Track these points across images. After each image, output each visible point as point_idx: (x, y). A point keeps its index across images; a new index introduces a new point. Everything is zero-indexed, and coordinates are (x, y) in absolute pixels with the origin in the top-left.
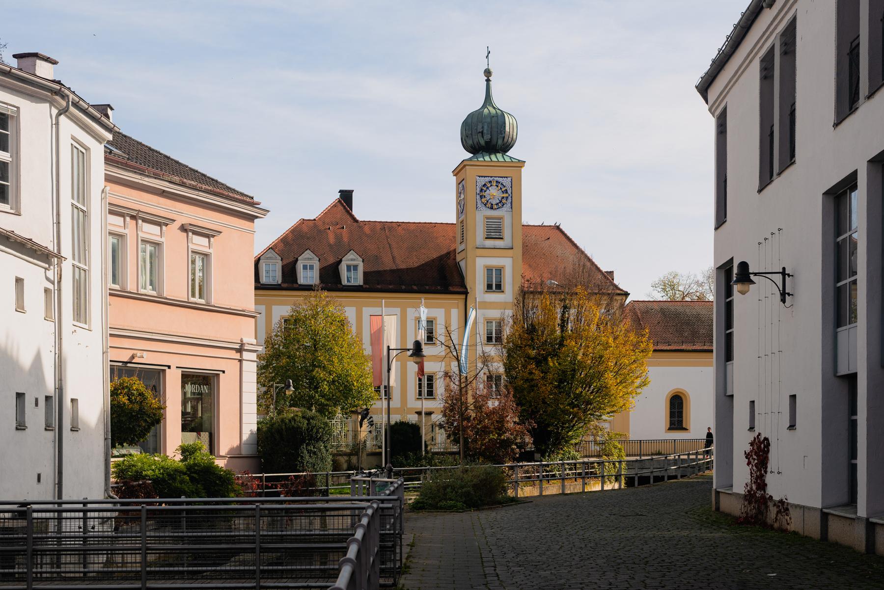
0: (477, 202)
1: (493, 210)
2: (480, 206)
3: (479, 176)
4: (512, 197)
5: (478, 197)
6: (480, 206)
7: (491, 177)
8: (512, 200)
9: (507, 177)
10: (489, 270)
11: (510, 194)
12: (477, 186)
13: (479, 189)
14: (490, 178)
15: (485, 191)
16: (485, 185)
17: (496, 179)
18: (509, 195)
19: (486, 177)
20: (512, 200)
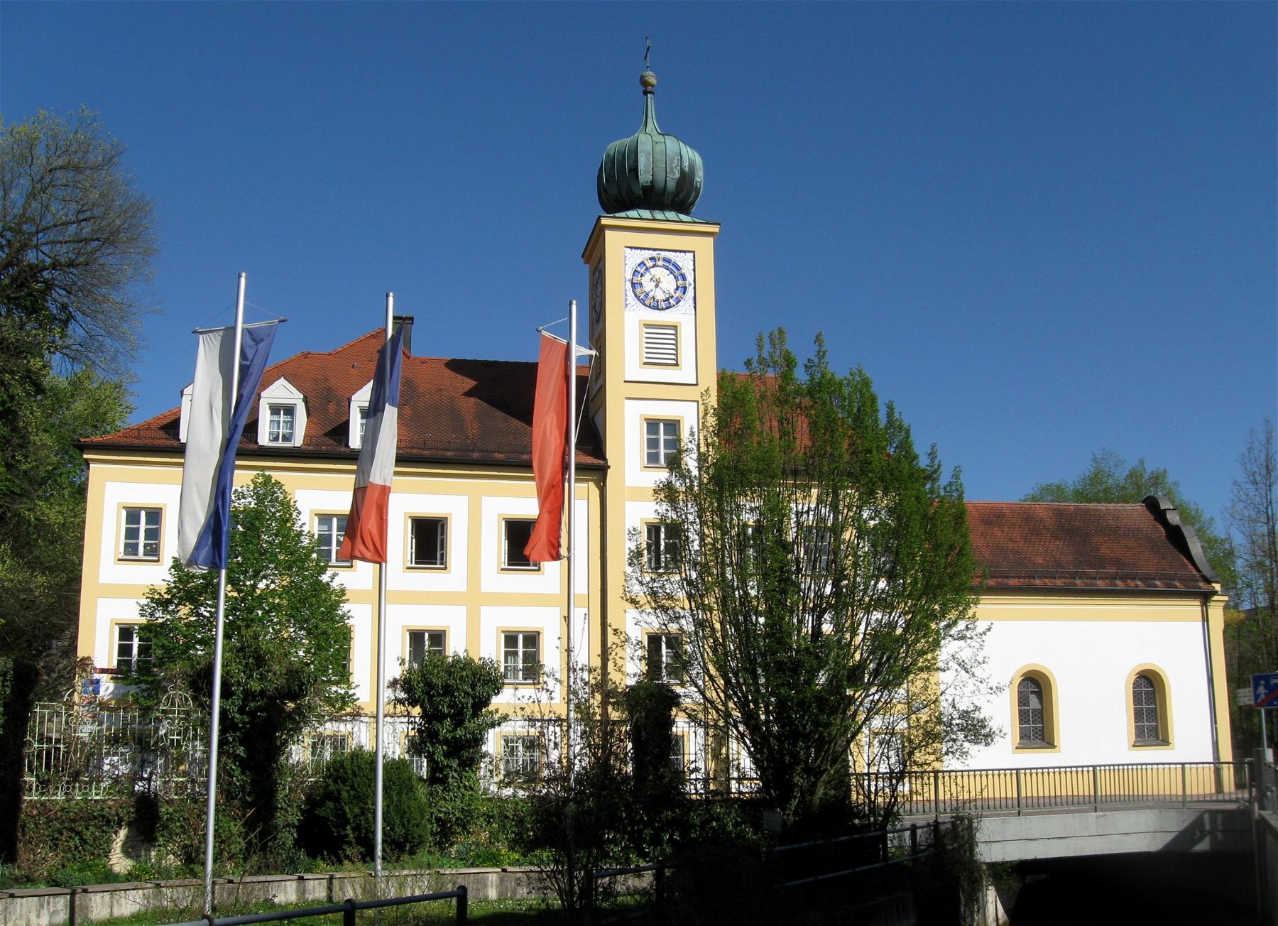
0: (626, 295)
1: (658, 311)
2: (633, 303)
3: (631, 248)
4: (695, 288)
5: (629, 285)
6: (633, 303)
8: (695, 293)
9: (685, 252)
10: (652, 425)
11: (692, 282)
14: (651, 251)
15: (642, 275)
16: (642, 263)
17: (663, 254)
18: (690, 285)
19: (645, 249)
20: (695, 293)
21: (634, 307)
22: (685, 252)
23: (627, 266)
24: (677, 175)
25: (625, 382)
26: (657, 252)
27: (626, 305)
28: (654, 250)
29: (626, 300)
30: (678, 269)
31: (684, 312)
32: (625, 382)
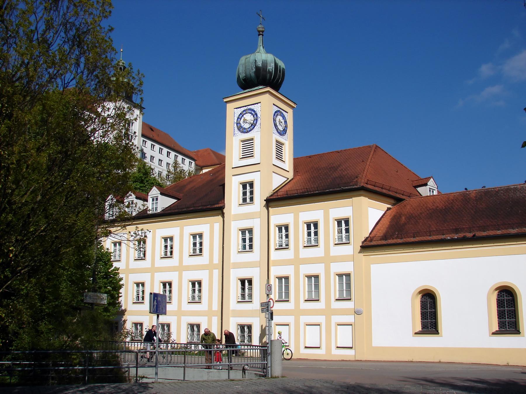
0: (234, 130)
2: (237, 133)
3: (237, 108)
7: (245, 106)
9: (257, 103)
12: (235, 116)
13: (236, 119)
14: (244, 108)
21: (237, 134)
22: (257, 103)
23: (235, 117)
24: (254, 70)
25: (233, 168)
26: (247, 107)
27: (234, 134)
28: (245, 106)
29: (234, 132)
30: (254, 111)
31: (256, 131)
32: (233, 168)
